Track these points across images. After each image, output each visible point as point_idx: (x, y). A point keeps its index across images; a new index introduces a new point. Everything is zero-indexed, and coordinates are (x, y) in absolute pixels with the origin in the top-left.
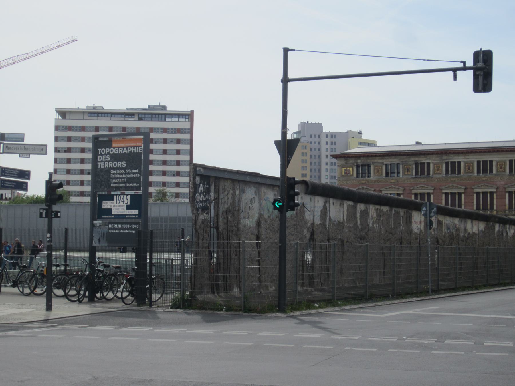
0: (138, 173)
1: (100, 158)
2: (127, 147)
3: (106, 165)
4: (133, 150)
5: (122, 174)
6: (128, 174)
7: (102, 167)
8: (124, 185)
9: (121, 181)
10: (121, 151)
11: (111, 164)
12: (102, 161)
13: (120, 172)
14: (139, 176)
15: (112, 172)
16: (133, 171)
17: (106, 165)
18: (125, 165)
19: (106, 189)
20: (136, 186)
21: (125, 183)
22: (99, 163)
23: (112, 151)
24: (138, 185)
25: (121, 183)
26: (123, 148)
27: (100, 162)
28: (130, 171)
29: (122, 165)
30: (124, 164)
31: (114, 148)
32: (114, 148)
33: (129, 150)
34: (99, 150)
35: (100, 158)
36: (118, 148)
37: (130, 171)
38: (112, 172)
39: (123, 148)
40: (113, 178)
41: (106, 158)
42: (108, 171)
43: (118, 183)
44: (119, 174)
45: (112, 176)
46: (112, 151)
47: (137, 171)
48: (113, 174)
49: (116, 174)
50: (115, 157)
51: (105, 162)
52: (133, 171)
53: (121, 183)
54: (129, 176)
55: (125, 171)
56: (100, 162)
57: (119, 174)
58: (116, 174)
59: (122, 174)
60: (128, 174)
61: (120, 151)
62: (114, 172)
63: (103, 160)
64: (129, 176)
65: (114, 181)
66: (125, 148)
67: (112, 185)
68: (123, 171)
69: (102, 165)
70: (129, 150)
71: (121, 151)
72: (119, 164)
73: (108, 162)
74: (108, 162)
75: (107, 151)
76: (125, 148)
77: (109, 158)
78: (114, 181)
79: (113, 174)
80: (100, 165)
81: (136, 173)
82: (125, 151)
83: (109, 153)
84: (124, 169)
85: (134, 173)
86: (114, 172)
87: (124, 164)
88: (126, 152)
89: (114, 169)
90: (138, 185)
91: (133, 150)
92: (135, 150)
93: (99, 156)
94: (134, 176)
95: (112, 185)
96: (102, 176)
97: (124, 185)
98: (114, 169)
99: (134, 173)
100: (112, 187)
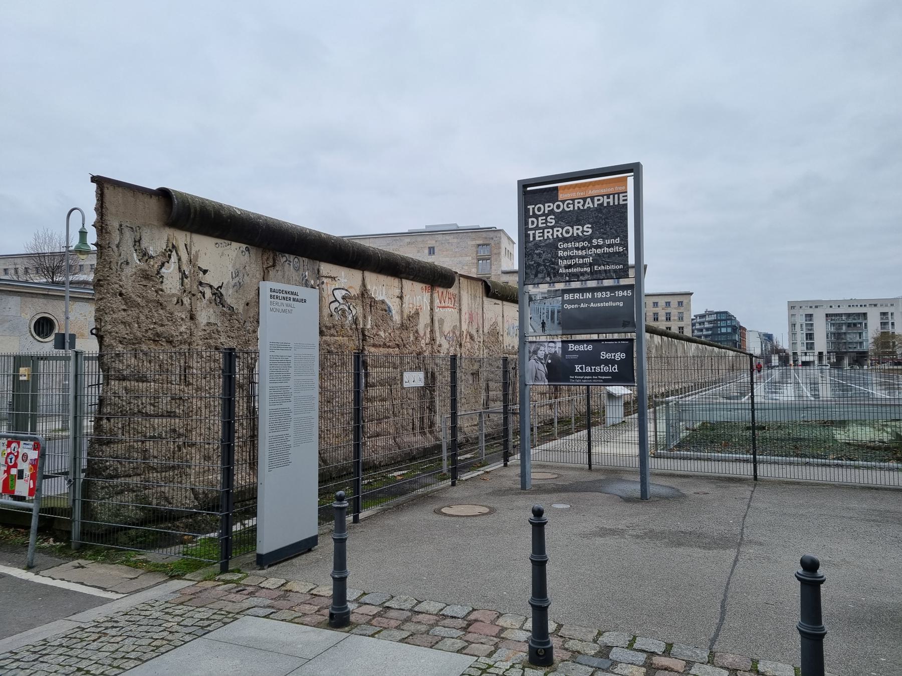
0: (619, 245)
1: (533, 223)
2: (592, 198)
4: (606, 200)
5: (583, 248)
6: (597, 247)
7: (537, 239)
8: (588, 270)
9: (581, 261)
10: (578, 205)
11: (558, 232)
12: (537, 228)
13: (581, 244)
14: (621, 249)
15: (561, 245)
16: (608, 242)
17: (546, 234)
18: (590, 230)
19: (548, 279)
20: (615, 271)
21: (591, 265)
22: (531, 233)
24: (621, 266)
25: (582, 266)
26: (585, 199)
28: (601, 242)
29: (583, 231)
30: (588, 229)
31: (563, 202)
33: (596, 203)
34: (531, 207)
35: (533, 223)
36: (573, 200)
37: (601, 242)
38: (561, 245)
40: (561, 258)
42: (553, 246)
43: (576, 265)
44: (577, 249)
45: (560, 253)
48: (565, 250)
49: (571, 249)
50: (564, 218)
51: (543, 229)
52: (608, 242)
53: (582, 266)
54: (599, 251)
55: (590, 242)
56: (531, 229)
57: (577, 249)
58: (571, 249)
59: (583, 248)
60: (597, 247)
61: (576, 205)
62: (565, 246)
63: (540, 225)
64: (599, 251)
66: (589, 200)
68: (586, 244)
69: (537, 235)
70: (596, 203)
71: (580, 205)
72: (577, 230)
73: (552, 228)
74: (552, 228)
75: (547, 209)
76: (589, 200)
77: (553, 221)
79: (565, 250)
80: (534, 234)
81: (616, 245)
82: (589, 204)
83: (551, 212)
84: (589, 239)
85: (609, 246)
86: (565, 246)
87: (588, 229)
89: (565, 240)
90: (621, 266)
91: (606, 200)
92: (611, 200)
93: (530, 220)
94: (611, 250)
96: (539, 255)
97: (588, 270)
98: (565, 240)
99: (609, 246)
100: (562, 274)
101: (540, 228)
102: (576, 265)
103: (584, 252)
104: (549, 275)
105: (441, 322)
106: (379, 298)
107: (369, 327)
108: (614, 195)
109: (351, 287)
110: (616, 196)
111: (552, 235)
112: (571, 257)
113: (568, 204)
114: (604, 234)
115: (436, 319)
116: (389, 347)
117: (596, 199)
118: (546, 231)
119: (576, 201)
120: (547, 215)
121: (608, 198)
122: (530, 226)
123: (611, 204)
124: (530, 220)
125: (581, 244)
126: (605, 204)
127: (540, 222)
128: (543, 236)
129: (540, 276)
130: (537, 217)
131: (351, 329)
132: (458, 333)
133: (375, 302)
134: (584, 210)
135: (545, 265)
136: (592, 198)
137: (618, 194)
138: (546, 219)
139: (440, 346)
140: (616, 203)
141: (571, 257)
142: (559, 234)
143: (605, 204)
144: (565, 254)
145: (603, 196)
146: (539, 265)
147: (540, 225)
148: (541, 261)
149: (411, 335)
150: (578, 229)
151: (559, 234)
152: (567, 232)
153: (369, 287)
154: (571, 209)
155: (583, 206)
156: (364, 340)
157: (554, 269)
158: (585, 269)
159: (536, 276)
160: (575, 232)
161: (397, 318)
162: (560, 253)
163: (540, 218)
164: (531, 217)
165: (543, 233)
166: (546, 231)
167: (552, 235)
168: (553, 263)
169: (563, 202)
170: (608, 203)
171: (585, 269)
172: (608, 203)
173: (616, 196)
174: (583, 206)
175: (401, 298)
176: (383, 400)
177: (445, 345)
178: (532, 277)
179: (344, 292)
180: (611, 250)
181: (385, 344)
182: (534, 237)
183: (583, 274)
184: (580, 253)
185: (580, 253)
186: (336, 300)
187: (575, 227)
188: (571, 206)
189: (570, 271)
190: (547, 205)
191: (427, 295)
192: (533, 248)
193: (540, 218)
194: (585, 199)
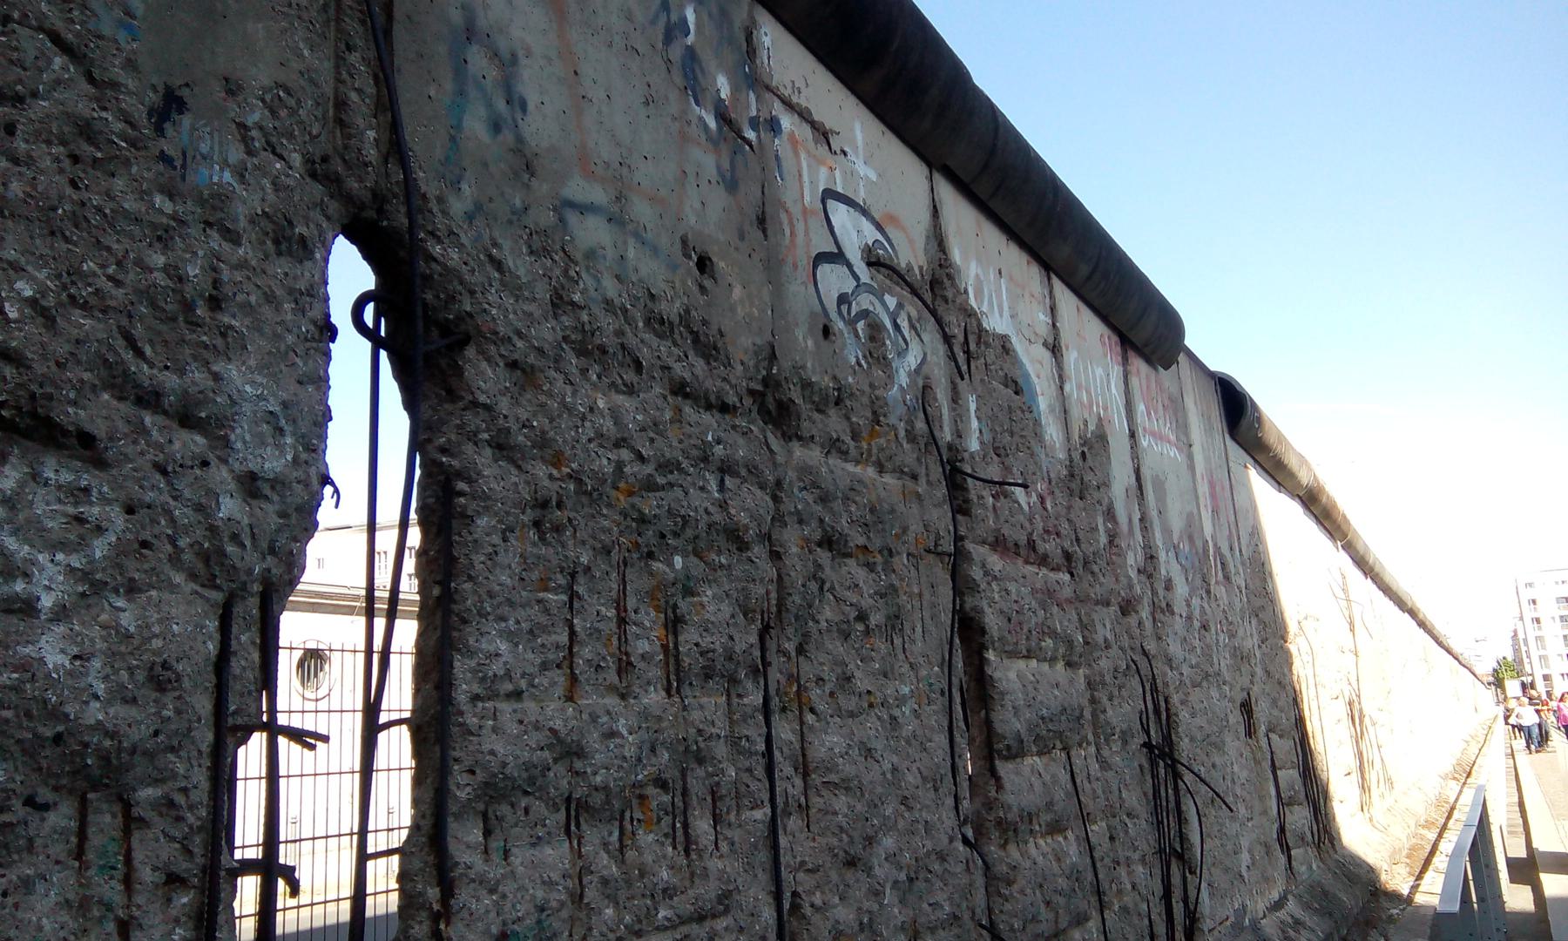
105: (1159, 485)
106: (997, 323)
107: (974, 445)
109: (893, 219)
115: (1146, 473)
116: (1043, 561)
131: (911, 437)
132: (1199, 544)
133: (981, 331)
139: (1169, 586)
149: (1100, 520)
153: (956, 256)
156: (960, 506)
161: (1052, 432)
175: (1055, 349)
176: (1055, 828)
177: (1181, 589)
179: (871, 234)
181: (1031, 545)
186: (837, 256)
191: (1116, 371)
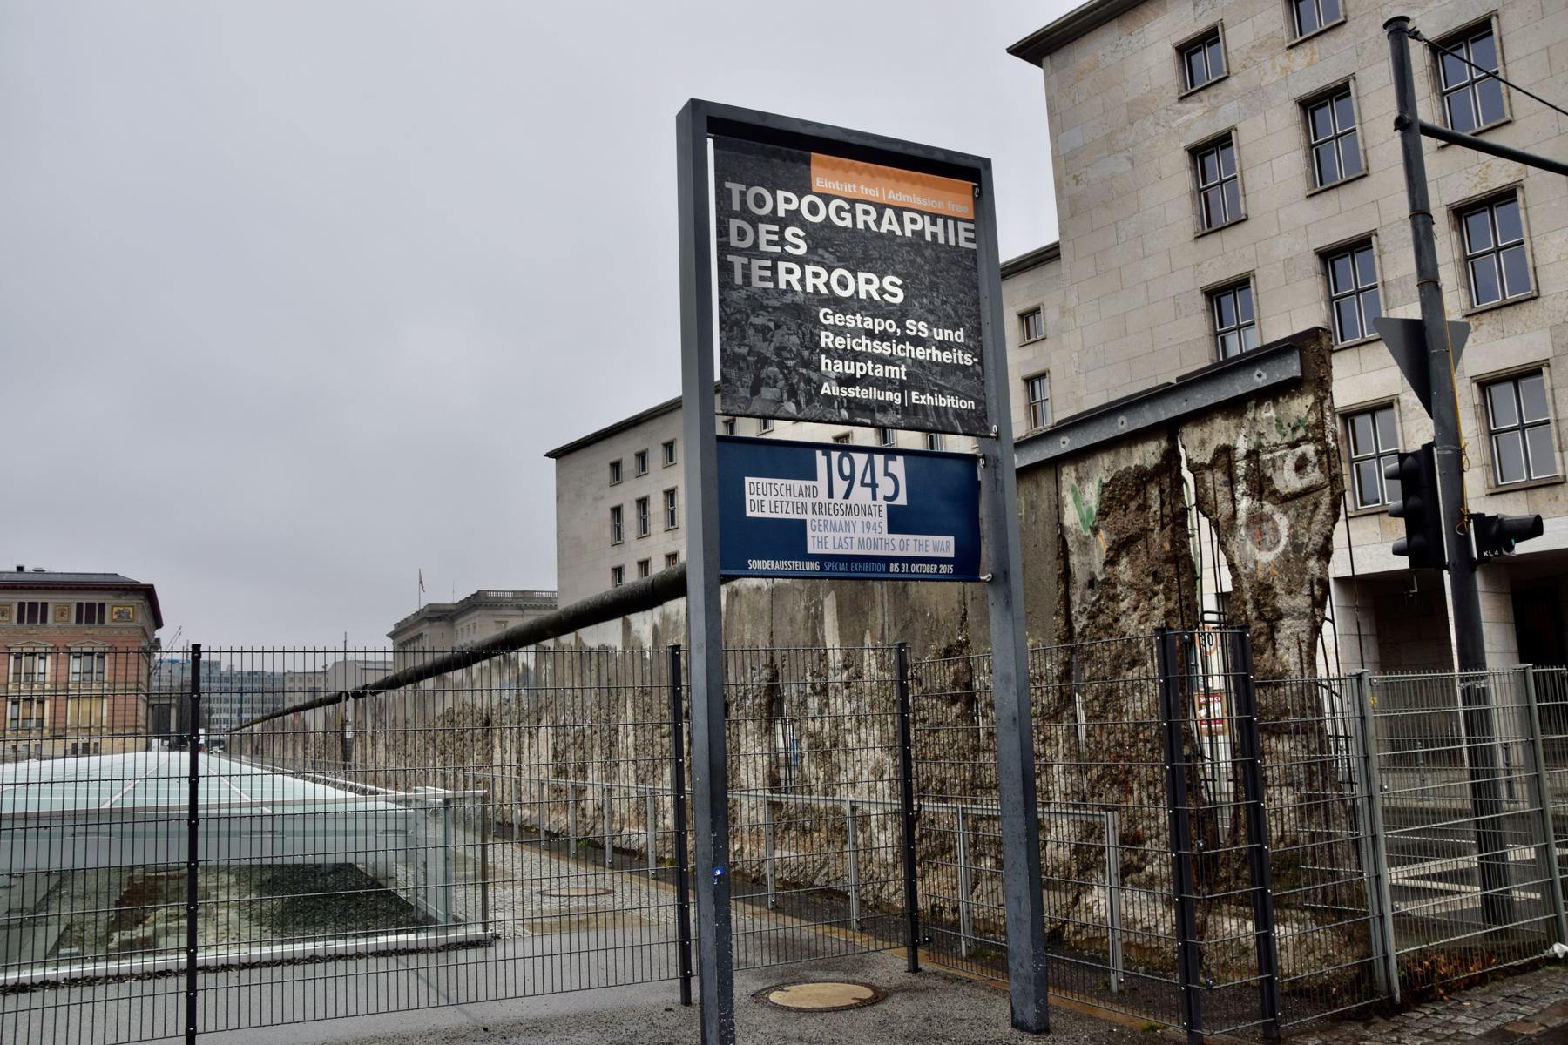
0: (964, 348)
1: (742, 234)
2: (899, 211)
3: (788, 276)
5: (884, 337)
6: (917, 341)
7: (756, 283)
8: (896, 398)
9: (880, 371)
10: (865, 218)
11: (816, 279)
13: (880, 325)
14: (969, 360)
16: (939, 335)
17: (783, 278)
19: (791, 407)
20: (958, 413)
21: (902, 387)
22: (738, 261)
23: (813, 209)
24: (971, 404)
25: (883, 384)
27: (738, 252)
29: (882, 291)
32: (827, 198)
34: (735, 188)
35: (742, 234)
36: (852, 202)
39: (881, 208)
40: (827, 352)
41: (782, 241)
43: (866, 381)
44: (870, 334)
45: (826, 339)
46: (813, 209)
47: (959, 336)
48: (839, 331)
49: (856, 333)
51: (776, 259)
52: (939, 335)
54: (921, 353)
56: (738, 252)
57: (870, 334)
58: (856, 333)
59: (884, 337)
60: (917, 341)
64: (921, 353)
65: (839, 367)
66: (889, 213)
67: (826, 389)
68: (890, 326)
69: (756, 273)
70: (909, 228)
72: (865, 285)
74: (801, 261)
76: (889, 213)
78: (839, 367)
79: (839, 331)
80: (747, 270)
81: (959, 346)
82: (889, 225)
83: (794, 218)
84: (900, 315)
85: (943, 346)
86: (839, 319)
88: (896, 228)
89: (840, 305)
90: (971, 404)
91: (929, 229)
92: (939, 229)
94: (946, 357)
95: (826, 389)
96: (764, 331)
97: (896, 398)
98: (840, 305)
99: (943, 346)
100: (829, 399)
101: (765, 256)
102: (866, 381)
103: (885, 349)
104: (793, 394)
108: (946, 218)
110: (951, 223)
111: (802, 280)
112: (855, 356)
113: (839, 209)
114: (931, 312)
117: (907, 216)
118: (782, 266)
119: (860, 207)
120: (783, 224)
121: (934, 223)
122: (734, 241)
123: (941, 240)
124: (734, 224)
125: (880, 325)
126: (928, 238)
127: (763, 237)
128: (774, 278)
129: (767, 393)
130: (755, 221)
134: (880, 235)
135: (782, 366)
136: (899, 211)
137: (956, 220)
138: (781, 233)
140: (952, 242)
141: (855, 356)
142: (820, 283)
143: (928, 238)
144: (840, 343)
145: (922, 213)
146: (763, 361)
147: (763, 247)
148: (768, 350)
150: (869, 281)
151: (820, 283)
152: (843, 284)
154: (848, 223)
155: (878, 222)
157: (808, 381)
158: (890, 396)
159: (755, 391)
160: (863, 288)
162: (826, 339)
163: (763, 227)
164: (737, 216)
165: (774, 269)
166: (782, 266)
167: (802, 280)
168: (806, 364)
169: (827, 198)
170: (934, 235)
171: (890, 396)
172: (934, 235)
173: (951, 223)
174: (878, 222)
178: (744, 392)
180: (946, 357)
182: (747, 276)
183: (885, 407)
184: (877, 347)
185: (877, 347)
187: (862, 276)
188: (848, 216)
189: (853, 392)
190: (781, 194)
192: (744, 305)
193: (763, 227)
194: (881, 208)
